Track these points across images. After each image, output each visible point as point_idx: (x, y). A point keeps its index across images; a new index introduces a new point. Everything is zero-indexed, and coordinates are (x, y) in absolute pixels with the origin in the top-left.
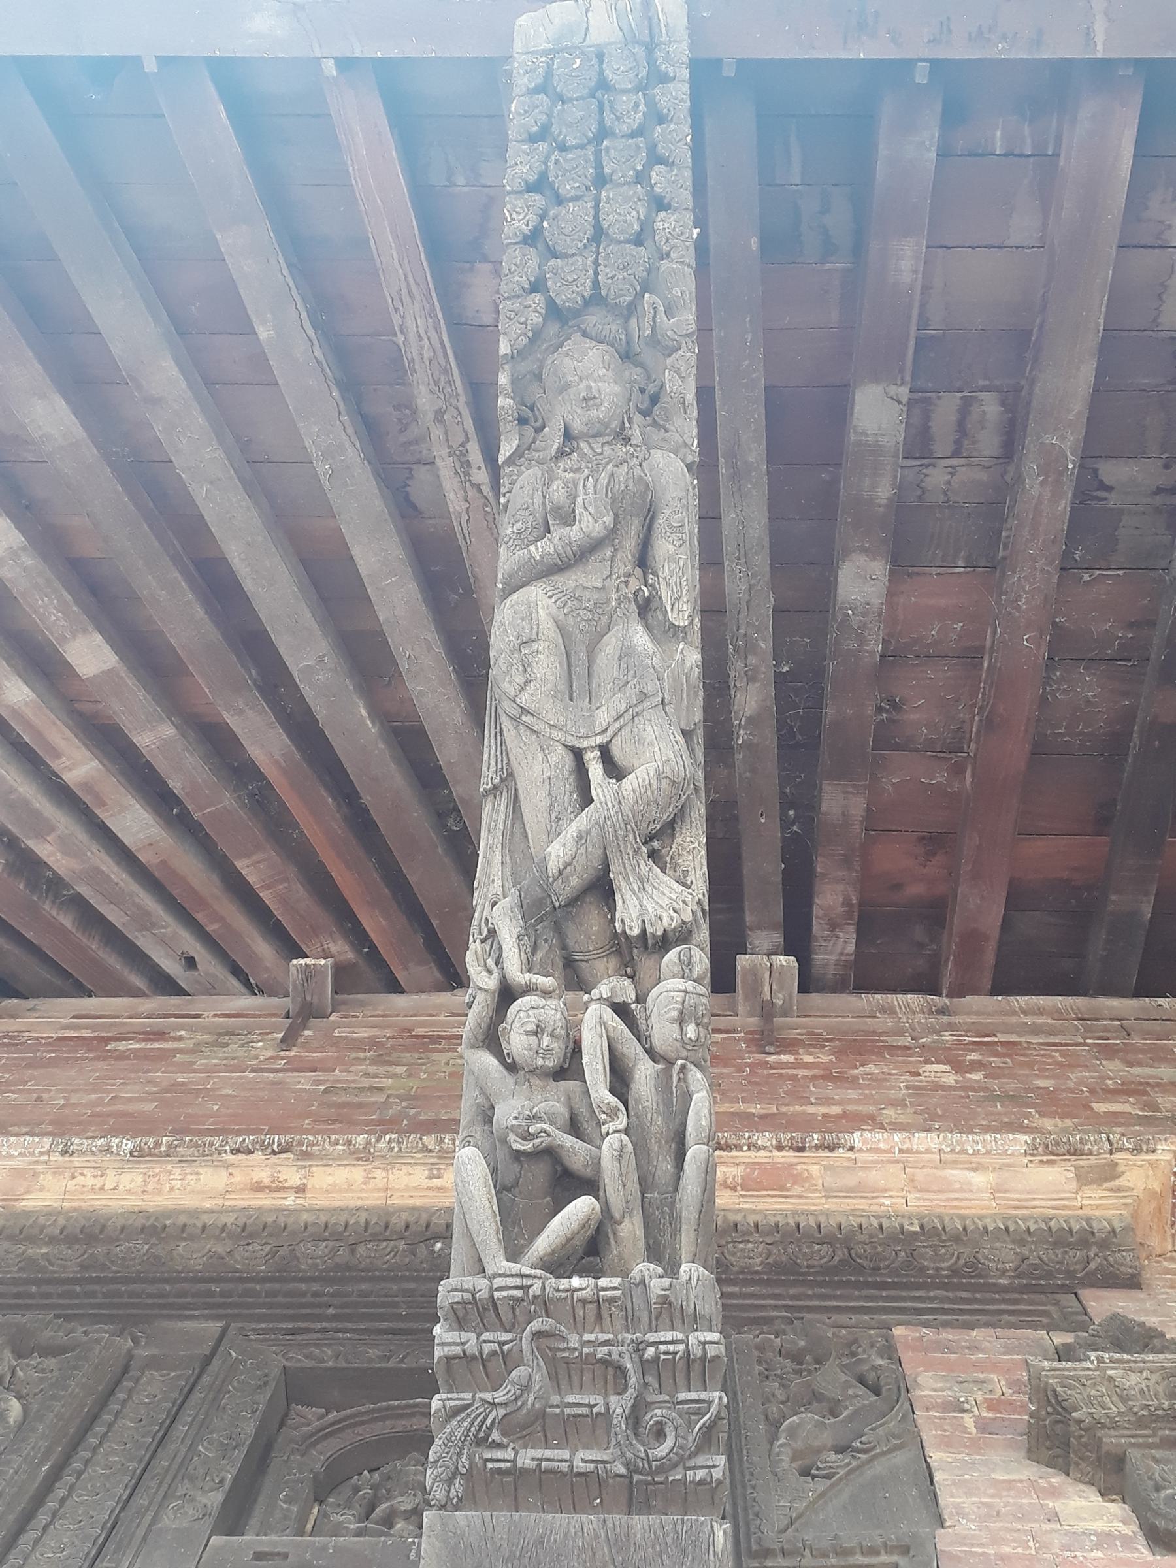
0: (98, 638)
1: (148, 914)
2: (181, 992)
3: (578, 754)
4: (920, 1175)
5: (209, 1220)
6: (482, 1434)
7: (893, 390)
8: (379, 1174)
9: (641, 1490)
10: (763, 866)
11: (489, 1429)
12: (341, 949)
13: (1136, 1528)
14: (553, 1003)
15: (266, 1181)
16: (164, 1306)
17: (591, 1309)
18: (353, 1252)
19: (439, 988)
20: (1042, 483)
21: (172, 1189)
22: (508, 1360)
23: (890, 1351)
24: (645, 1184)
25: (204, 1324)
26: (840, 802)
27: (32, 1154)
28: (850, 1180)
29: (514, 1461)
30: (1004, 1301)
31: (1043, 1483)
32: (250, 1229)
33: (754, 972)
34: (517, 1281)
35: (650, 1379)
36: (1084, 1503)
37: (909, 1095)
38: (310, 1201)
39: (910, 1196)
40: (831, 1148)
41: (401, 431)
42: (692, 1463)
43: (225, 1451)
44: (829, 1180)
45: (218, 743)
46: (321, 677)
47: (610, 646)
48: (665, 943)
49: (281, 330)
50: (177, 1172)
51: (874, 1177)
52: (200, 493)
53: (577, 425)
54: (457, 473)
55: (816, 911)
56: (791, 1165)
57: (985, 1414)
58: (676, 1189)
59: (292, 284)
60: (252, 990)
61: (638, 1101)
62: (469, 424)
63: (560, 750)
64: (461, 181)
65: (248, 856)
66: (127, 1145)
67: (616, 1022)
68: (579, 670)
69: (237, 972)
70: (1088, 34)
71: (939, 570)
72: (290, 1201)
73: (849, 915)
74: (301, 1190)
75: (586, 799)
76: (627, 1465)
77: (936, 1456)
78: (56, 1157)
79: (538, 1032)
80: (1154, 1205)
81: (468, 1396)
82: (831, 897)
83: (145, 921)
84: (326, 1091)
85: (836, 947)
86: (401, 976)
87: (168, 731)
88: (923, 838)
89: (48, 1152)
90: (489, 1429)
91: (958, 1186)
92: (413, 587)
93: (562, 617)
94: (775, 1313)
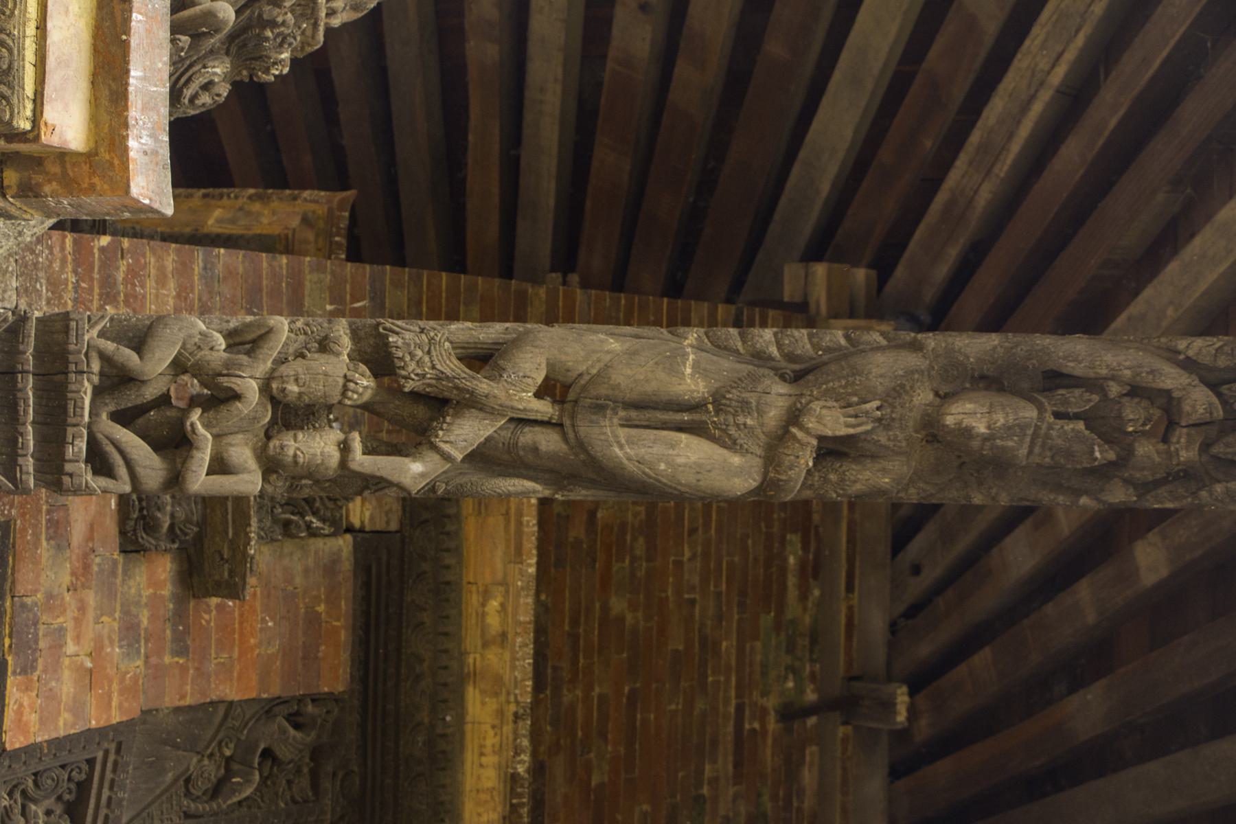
60: (893, 627)
66: (521, 769)
69: (913, 611)
78: (513, 708)
84: (699, 799)
89: (517, 702)
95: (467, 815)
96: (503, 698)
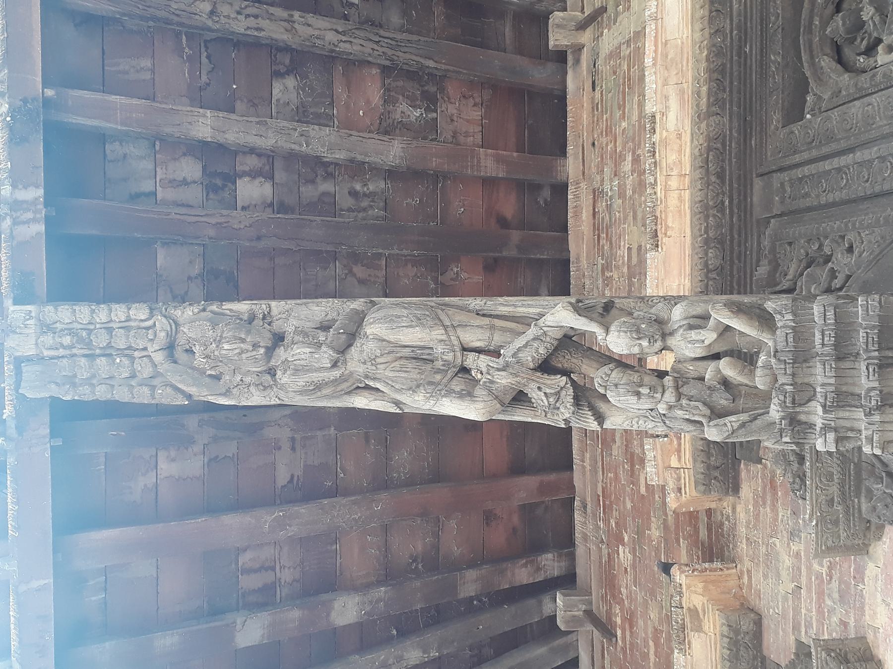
7: (239, 627)
20: (290, 526)
33: (567, 622)
70: (39, 590)
71: (338, 558)
73: (532, 562)
80: (711, 587)
82: (522, 575)
85: (550, 564)
88: (487, 523)
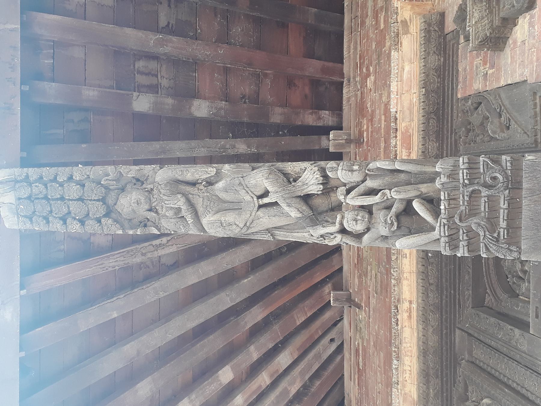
0: (220, 372)
1: (315, 355)
2: (342, 344)
3: (260, 207)
4: (405, 88)
5: (421, 334)
6: (495, 240)
7: (134, 98)
8: (405, 275)
9: (514, 185)
10: (299, 143)
11: (493, 237)
12: (327, 288)
13: (527, 14)
14: (346, 215)
15: (408, 314)
16: (451, 349)
17: (452, 202)
18: (432, 284)
19: (341, 254)
20: (167, 46)
21: (410, 347)
22: (469, 230)
23: (466, 99)
24: (409, 183)
25: (457, 335)
26: (277, 116)
27: (398, 395)
28: (407, 113)
29: (504, 229)
30: (449, 59)
31: (512, 46)
32: (424, 320)
33: (335, 146)
34: (442, 227)
35: (476, 182)
36: (519, 32)
37: (378, 92)
38: (414, 299)
39: (413, 92)
40: (396, 119)
41: (149, 268)
42: (505, 167)
43: (500, 328)
44: (407, 120)
45: (256, 331)
46: (234, 295)
47: (223, 196)
48: (325, 177)
49: (113, 309)
50: (404, 345)
51: (406, 104)
52: (170, 337)
53: (147, 207)
54: (163, 248)
55: (314, 124)
56: (402, 133)
57: (488, 66)
58: (410, 173)
59: (98, 305)
60: (342, 319)
61: (380, 186)
62: (146, 244)
63: (259, 213)
64: (62, 247)
65: (295, 321)
66: (395, 362)
67: (353, 193)
68: (231, 206)
69: (335, 324)
71: (197, 82)
72: (414, 306)
73: (316, 113)
74: (410, 302)
75: (276, 204)
76: (505, 190)
77: (502, 83)
78: (399, 387)
79: (356, 220)
80: (416, 8)
81: (482, 245)
82: (309, 119)
83: (318, 356)
84: (376, 293)
85: (327, 117)
86: (337, 268)
87: (252, 348)
88: (289, 87)
89: (398, 389)
90: (493, 237)
91: (409, 76)
92: (202, 263)
93: (213, 212)
94: (453, 138)
95: (415, 348)
96: (403, 392)
